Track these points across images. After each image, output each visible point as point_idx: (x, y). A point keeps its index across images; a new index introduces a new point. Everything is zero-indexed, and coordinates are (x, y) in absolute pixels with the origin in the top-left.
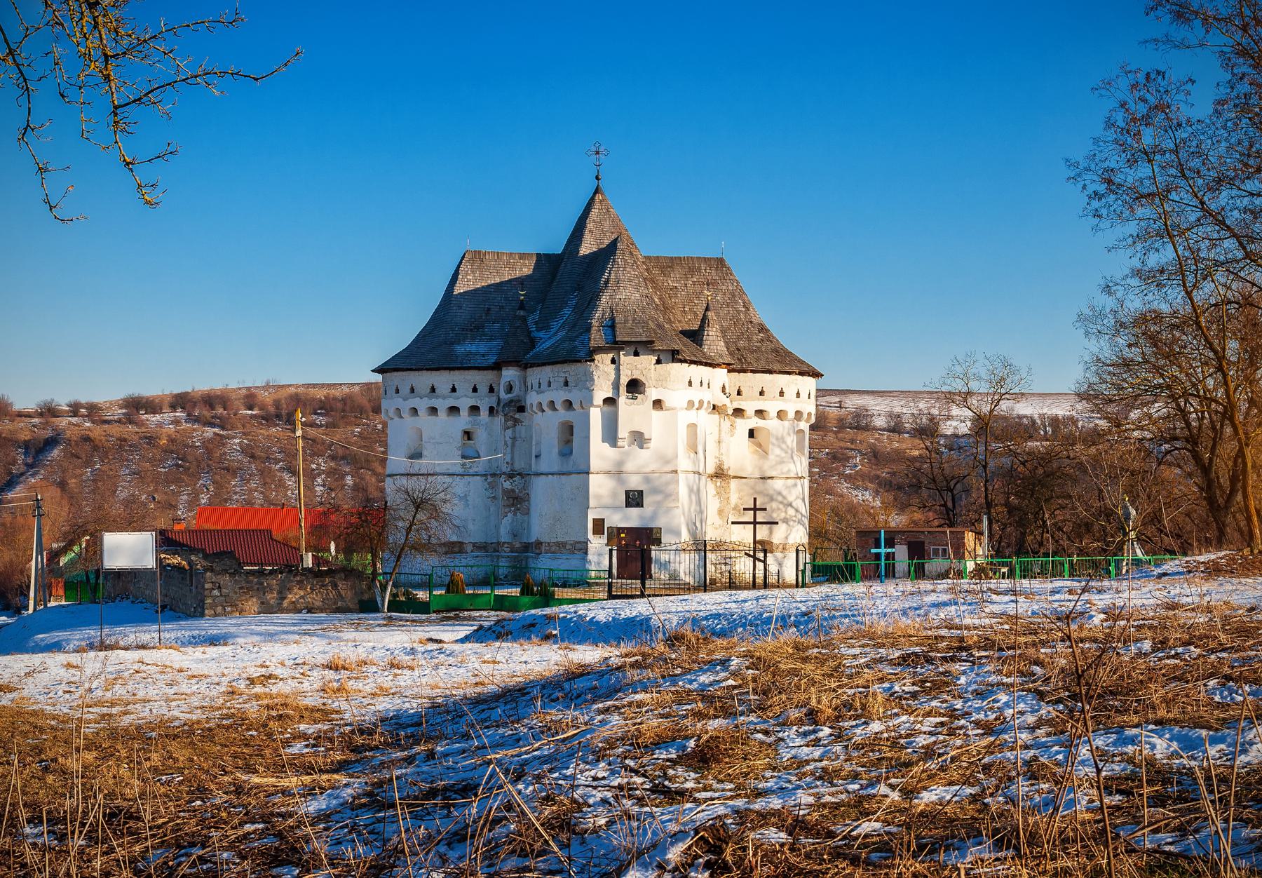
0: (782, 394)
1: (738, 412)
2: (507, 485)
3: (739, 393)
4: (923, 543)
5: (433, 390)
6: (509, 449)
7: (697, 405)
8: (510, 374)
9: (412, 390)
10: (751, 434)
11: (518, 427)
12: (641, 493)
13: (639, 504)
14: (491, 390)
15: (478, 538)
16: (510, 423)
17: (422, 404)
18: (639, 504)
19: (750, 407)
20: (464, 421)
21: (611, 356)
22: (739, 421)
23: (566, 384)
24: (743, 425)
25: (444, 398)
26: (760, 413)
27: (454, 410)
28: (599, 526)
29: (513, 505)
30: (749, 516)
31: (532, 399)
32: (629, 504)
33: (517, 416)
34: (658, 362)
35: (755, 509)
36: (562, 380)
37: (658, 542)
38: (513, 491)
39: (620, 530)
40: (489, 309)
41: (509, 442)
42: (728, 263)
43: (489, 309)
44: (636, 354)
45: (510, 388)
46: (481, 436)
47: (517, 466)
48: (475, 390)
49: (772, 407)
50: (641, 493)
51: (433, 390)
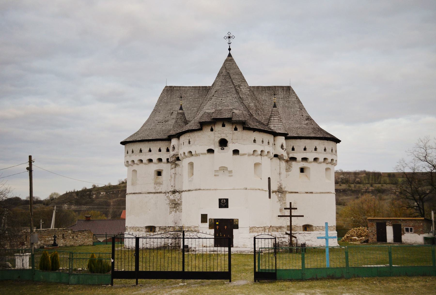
0: (316, 149)
2: (172, 197)
3: (293, 149)
4: (400, 225)
5: (141, 151)
6: (173, 180)
7: (259, 153)
8: (174, 142)
9: (133, 152)
10: (302, 170)
11: (177, 168)
12: (227, 200)
13: (226, 206)
14: (168, 150)
15: (162, 225)
16: (173, 166)
17: (136, 158)
18: (226, 206)
19: (299, 156)
20: (155, 167)
21: (210, 128)
22: (294, 163)
23: (189, 142)
24: (296, 166)
25: (145, 155)
26: (305, 159)
27: (150, 161)
28: (204, 218)
29: (175, 207)
30: (287, 213)
31: (181, 152)
32: (221, 206)
33: (177, 162)
34: (236, 129)
35: (291, 209)
36: (188, 141)
37: (237, 227)
38: (175, 200)
39: (216, 220)
40: (172, 113)
41: (173, 176)
42: (293, 87)
43: (172, 113)
44: (224, 126)
45: (174, 148)
46: (164, 174)
47: (177, 189)
48: (160, 150)
49: (311, 156)
50: (227, 200)
51: (141, 151)
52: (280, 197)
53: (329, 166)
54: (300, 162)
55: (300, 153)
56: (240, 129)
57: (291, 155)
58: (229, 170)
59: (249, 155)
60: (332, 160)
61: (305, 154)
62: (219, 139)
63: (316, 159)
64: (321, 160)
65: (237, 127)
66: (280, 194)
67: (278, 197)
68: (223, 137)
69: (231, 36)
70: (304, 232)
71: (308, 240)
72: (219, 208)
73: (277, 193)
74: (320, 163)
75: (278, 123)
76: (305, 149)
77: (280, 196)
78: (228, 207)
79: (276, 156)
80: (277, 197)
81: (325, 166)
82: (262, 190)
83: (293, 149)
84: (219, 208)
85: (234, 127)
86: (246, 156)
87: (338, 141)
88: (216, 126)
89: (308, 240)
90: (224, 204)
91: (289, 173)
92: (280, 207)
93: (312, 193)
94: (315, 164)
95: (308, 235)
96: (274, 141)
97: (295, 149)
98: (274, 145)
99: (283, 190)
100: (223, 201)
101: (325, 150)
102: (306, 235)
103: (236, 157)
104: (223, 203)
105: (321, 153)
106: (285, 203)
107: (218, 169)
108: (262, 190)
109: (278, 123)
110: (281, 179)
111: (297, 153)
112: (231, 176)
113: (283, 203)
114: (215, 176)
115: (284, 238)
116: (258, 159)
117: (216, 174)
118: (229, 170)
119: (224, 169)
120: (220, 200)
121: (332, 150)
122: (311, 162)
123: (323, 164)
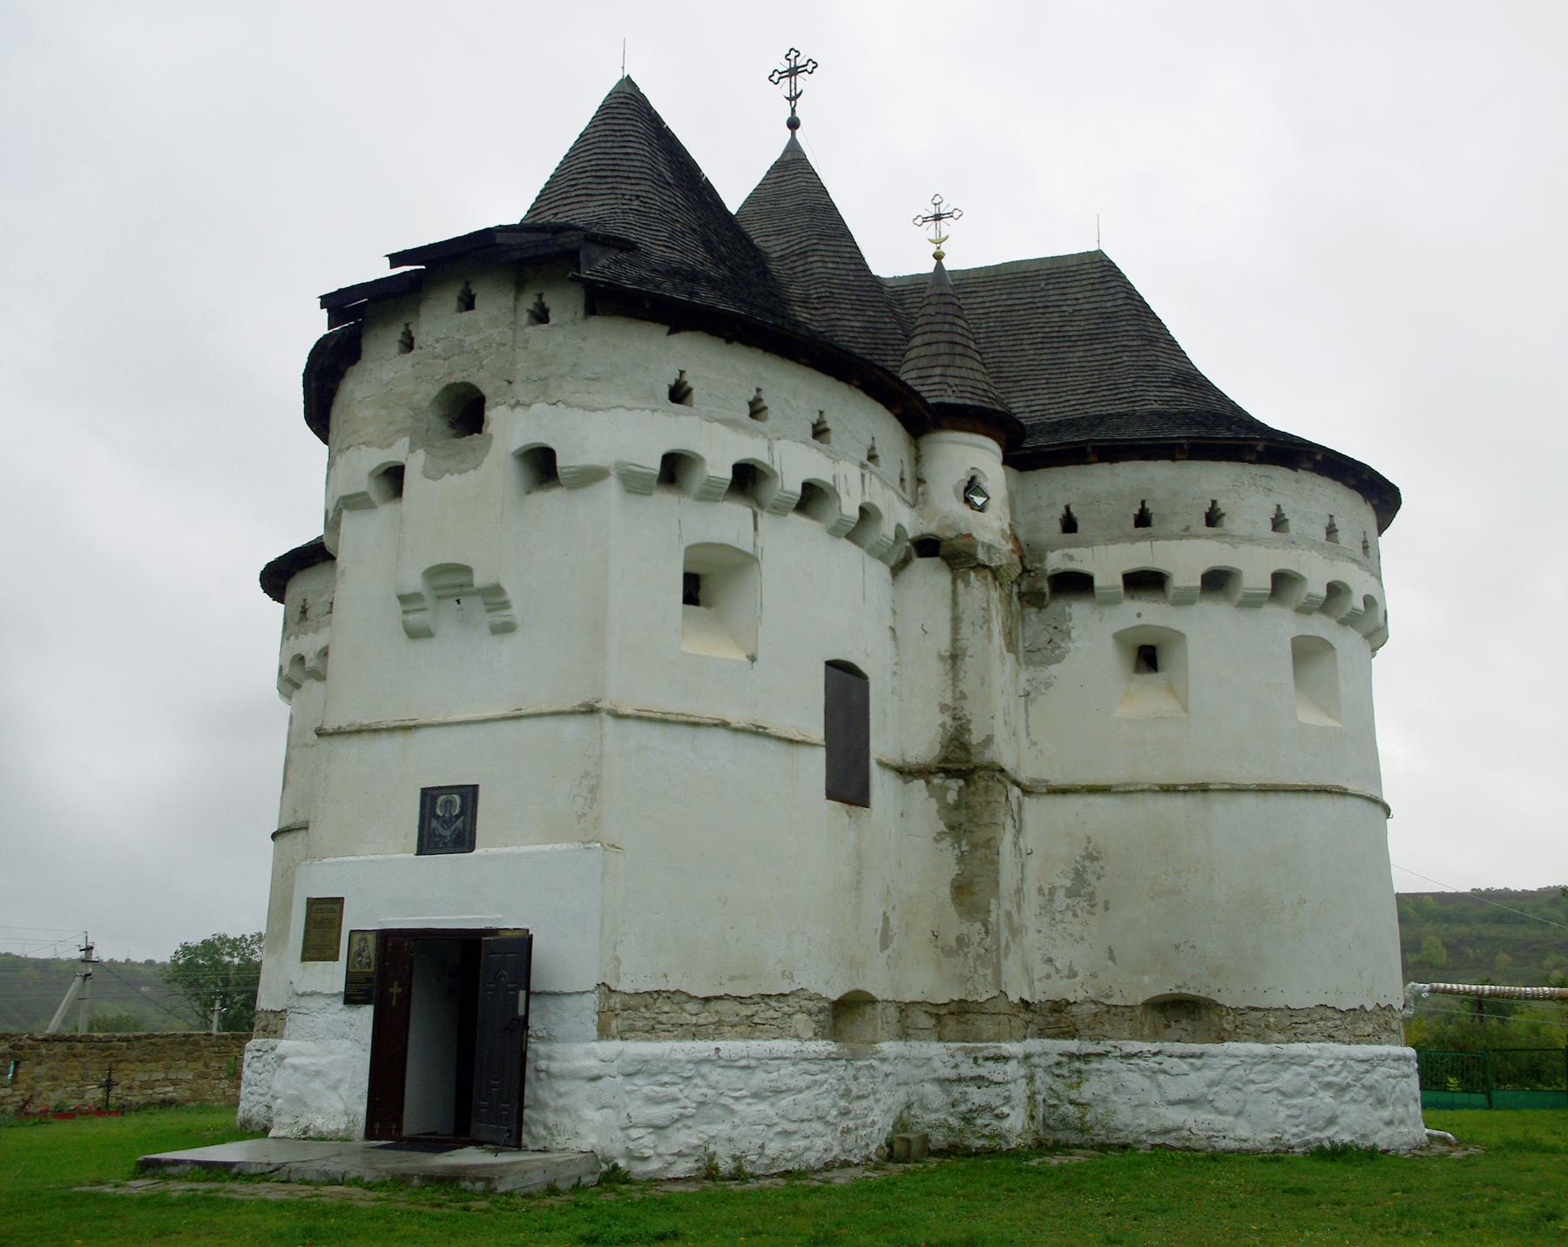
0: (1213, 518)
1: (1076, 584)
3: (1069, 524)
10: (1147, 658)
12: (470, 794)
13: (464, 841)
18: (464, 841)
19: (1107, 562)
21: (395, 334)
22: (1078, 611)
24: (1094, 632)
26: (1145, 582)
32: (428, 843)
34: (541, 316)
39: (388, 938)
44: (468, 303)
49: (1185, 560)
50: (470, 794)
52: (956, 807)
53: (1320, 626)
54: (1112, 601)
55: (1112, 540)
56: (564, 304)
57: (1056, 561)
58: (480, 580)
59: (633, 482)
60: (1336, 590)
61: (1143, 546)
62: (435, 390)
63: (1217, 581)
64: (1256, 578)
65: (550, 301)
66: (955, 784)
67: (947, 810)
68: (458, 377)
69: (801, 61)
70: (1154, 1047)
71: (1189, 1102)
72: (422, 850)
73: (937, 781)
74: (1251, 602)
75: (945, 360)
76: (1143, 519)
77: (952, 797)
78: (471, 847)
79: (927, 547)
80: (933, 804)
81: (1282, 624)
82: (758, 732)
83: (1069, 524)
84: (422, 850)
85: (529, 302)
86: (611, 489)
87: (1381, 497)
88: (422, 309)
89: (1189, 1102)
90: (448, 822)
91: (1054, 669)
92: (955, 870)
93: (1204, 789)
94: (1215, 614)
95: (1183, 1066)
96: (918, 459)
97: (1081, 526)
98: (920, 481)
99: (976, 760)
100: (450, 802)
101: (1279, 523)
102: (1168, 1063)
103: (550, 499)
104: (446, 822)
105: (1250, 539)
106: (990, 845)
107: (414, 582)
108: (758, 732)
109: (945, 360)
110: (962, 687)
111: (1089, 544)
112: (506, 628)
113: (974, 847)
114: (416, 633)
115: (979, 1081)
116: (730, 523)
117: (415, 618)
118: (480, 580)
119: (450, 581)
120: (429, 796)
121: (1331, 531)
122: (1184, 599)
123: (1270, 610)
